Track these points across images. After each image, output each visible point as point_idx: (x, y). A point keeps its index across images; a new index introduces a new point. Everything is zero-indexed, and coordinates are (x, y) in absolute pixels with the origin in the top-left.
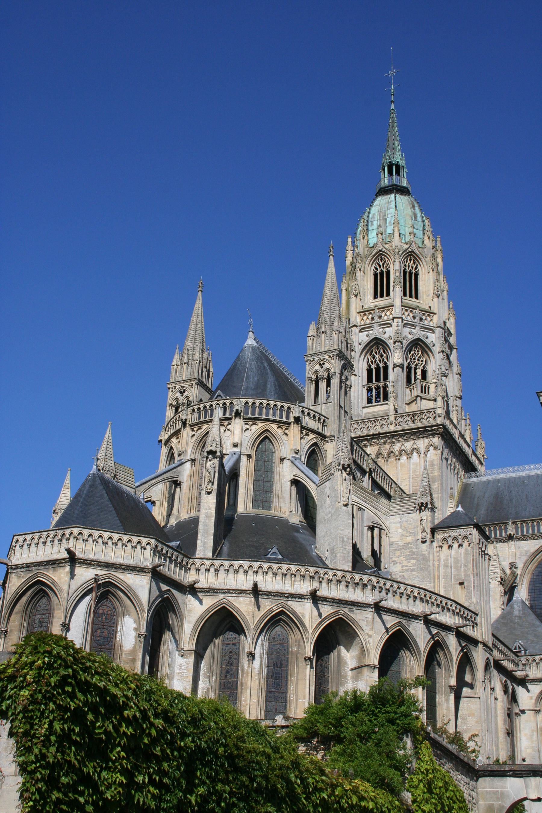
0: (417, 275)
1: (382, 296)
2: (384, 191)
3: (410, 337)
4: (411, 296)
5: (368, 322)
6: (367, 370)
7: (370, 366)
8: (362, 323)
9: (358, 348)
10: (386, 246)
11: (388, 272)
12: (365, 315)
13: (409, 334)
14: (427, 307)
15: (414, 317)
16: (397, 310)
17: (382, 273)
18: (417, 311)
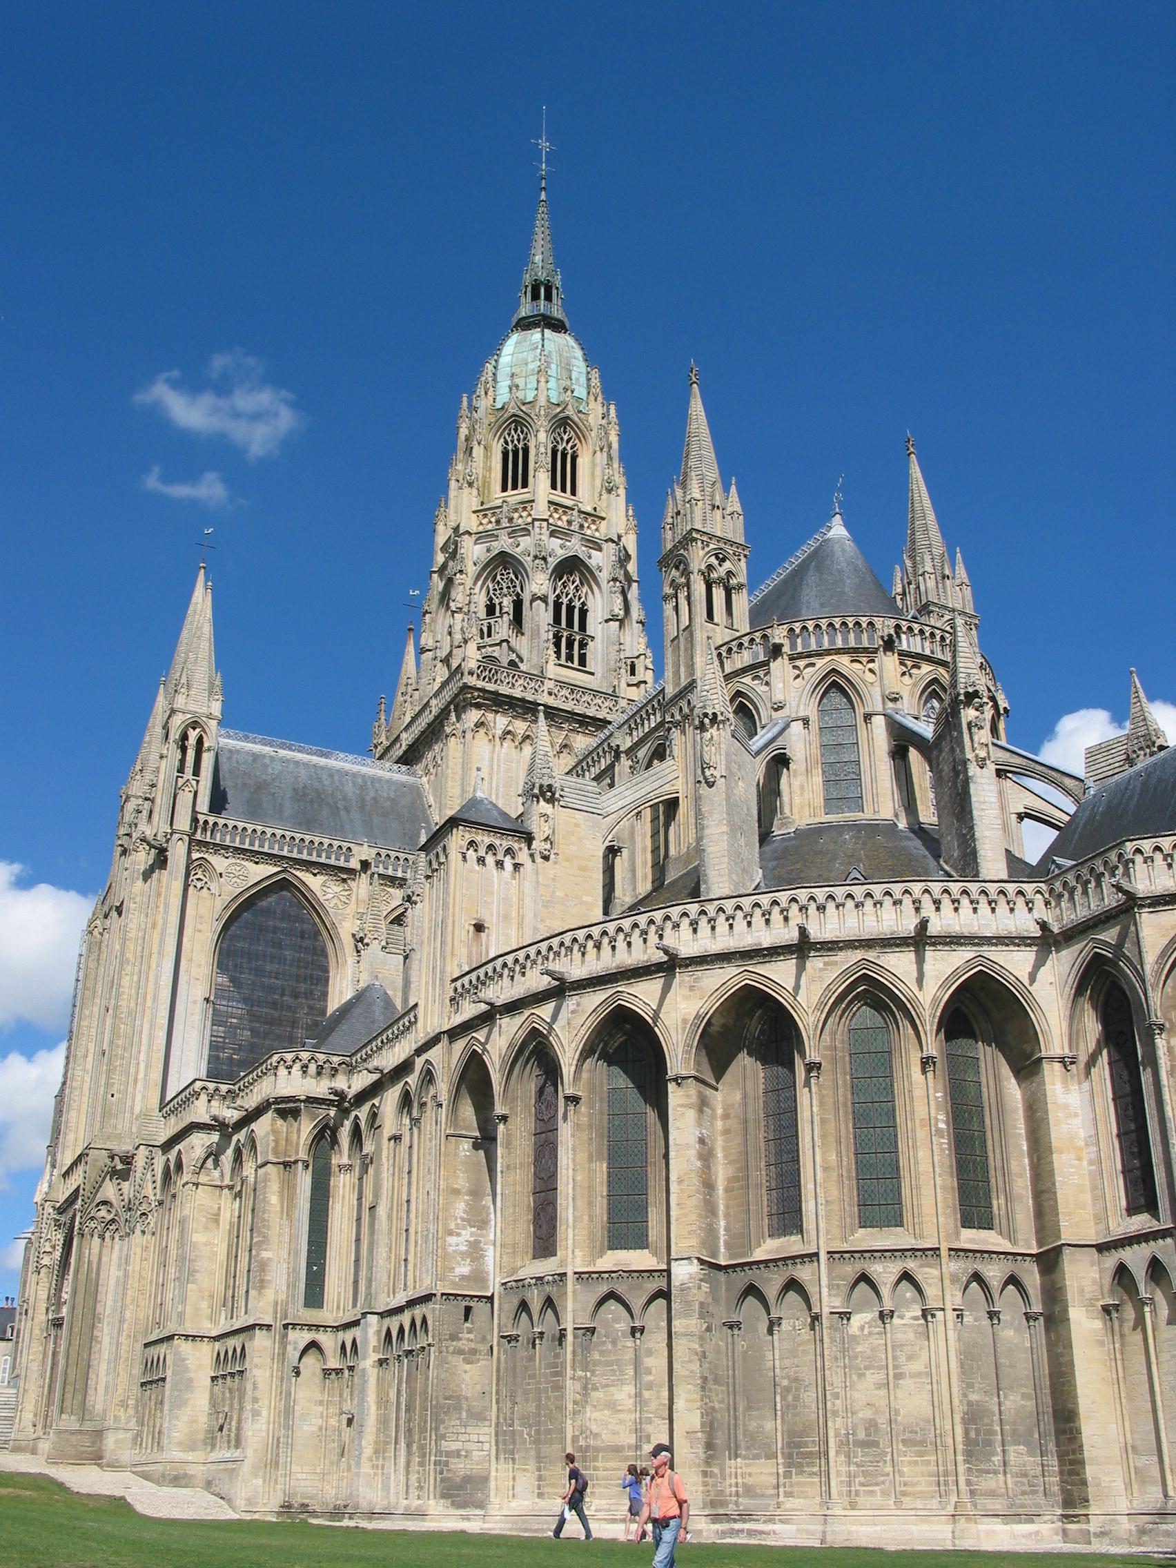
0: (574, 458)
1: (515, 487)
2: (525, 324)
4: (564, 490)
5: (490, 527)
7: (491, 599)
8: (481, 528)
9: (472, 570)
10: (523, 408)
11: (526, 450)
12: (485, 516)
13: (558, 549)
14: (589, 509)
15: (570, 523)
16: (541, 509)
18: (575, 513)
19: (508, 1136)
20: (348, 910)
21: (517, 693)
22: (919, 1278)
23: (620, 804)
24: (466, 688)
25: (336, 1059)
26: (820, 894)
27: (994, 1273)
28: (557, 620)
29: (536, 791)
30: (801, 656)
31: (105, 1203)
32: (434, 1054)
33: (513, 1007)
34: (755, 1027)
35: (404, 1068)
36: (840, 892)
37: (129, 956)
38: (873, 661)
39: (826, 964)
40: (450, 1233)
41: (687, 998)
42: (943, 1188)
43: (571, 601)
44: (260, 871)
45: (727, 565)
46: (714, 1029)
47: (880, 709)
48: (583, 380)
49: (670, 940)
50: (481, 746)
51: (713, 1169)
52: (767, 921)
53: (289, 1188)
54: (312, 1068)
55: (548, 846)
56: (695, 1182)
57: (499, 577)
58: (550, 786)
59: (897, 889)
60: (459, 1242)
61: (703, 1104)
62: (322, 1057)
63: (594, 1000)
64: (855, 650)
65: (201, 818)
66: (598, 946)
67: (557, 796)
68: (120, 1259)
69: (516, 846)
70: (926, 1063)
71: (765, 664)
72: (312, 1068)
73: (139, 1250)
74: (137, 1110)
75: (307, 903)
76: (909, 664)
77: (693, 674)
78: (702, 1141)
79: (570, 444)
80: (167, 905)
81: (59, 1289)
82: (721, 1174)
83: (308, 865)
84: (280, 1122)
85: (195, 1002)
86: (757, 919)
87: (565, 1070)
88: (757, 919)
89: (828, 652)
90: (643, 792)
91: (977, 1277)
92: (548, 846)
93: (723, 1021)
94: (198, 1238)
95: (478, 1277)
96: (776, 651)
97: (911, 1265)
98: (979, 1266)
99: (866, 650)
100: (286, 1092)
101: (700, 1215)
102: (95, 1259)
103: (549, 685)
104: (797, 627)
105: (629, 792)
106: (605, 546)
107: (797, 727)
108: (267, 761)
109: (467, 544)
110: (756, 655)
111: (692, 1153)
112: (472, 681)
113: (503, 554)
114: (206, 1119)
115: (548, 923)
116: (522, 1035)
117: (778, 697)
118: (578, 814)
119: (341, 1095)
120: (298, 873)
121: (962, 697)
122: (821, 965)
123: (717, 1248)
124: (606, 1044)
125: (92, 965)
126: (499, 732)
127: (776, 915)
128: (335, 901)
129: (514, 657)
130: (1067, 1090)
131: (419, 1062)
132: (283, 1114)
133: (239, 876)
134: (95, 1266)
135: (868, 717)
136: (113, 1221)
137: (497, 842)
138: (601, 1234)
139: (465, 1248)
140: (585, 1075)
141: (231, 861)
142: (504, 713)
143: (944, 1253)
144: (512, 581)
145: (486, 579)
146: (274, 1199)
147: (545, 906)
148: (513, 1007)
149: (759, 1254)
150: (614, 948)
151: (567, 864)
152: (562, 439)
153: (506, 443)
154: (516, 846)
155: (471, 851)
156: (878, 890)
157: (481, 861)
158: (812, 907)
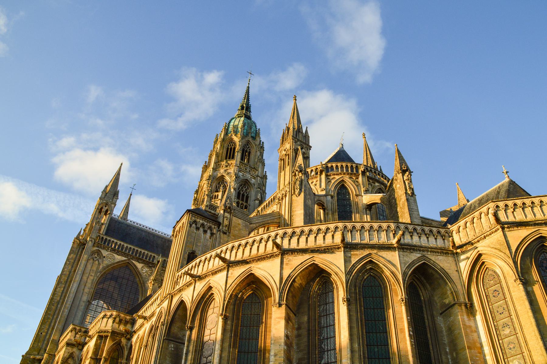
25: (128, 317)
34: (315, 287)
44: (119, 258)
46: (296, 285)
55: (227, 229)
61: (288, 319)
62: (122, 315)
65: (101, 236)
67: (232, 211)
69: (213, 226)
72: (118, 320)
83: (138, 260)
85: (84, 302)
93: (300, 282)
120: (134, 262)
124: (243, 294)
137: (206, 223)
154: (213, 226)
155: (194, 225)
157: (198, 229)
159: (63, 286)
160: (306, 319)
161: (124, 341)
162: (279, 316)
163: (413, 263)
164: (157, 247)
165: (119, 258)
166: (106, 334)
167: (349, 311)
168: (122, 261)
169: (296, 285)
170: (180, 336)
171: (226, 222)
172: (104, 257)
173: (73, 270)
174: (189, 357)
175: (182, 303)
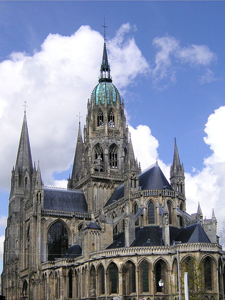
0: (114, 117)
3: (111, 142)
6: (96, 155)
11: (103, 116)
17: (100, 116)
18: (114, 133)
19: (97, 277)
20: (71, 225)
21: (102, 178)
22: (150, 299)
23: (116, 221)
24: (91, 177)
25: (72, 259)
26: (139, 248)
27: (161, 298)
28: (110, 158)
29: (102, 221)
30: (145, 197)
31: (33, 280)
32: (87, 263)
33: (98, 259)
35: (83, 264)
36: (142, 248)
37: (32, 236)
38: (158, 197)
39: (139, 258)
40: (91, 290)
41: (121, 261)
42: (154, 287)
43: (113, 153)
44: (54, 219)
45: (135, 176)
47: (158, 206)
48: (115, 97)
49: (119, 253)
50: (96, 189)
51: (125, 283)
52: (132, 251)
53: (65, 280)
54: (68, 261)
55: (104, 230)
56: (122, 286)
57: (98, 148)
58: (104, 221)
59: (150, 248)
60: (92, 291)
61: (123, 276)
62: (69, 259)
63: (109, 260)
64: (155, 196)
65: (43, 210)
66: (109, 253)
67: (105, 222)
68: (36, 289)
70: (152, 271)
71: (140, 197)
72: (68, 261)
73: (40, 288)
74: (37, 263)
75: (63, 224)
76: (164, 197)
77: (128, 197)
78: (123, 280)
79: (112, 114)
80: (38, 228)
81: (23, 292)
82: (127, 284)
83: (63, 217)
84: (64, 270)
85: (45, 244)
86: (131, 251)
87: (105, 269)
88: (131, 251)
89: (150, 196)
90: (120, 218)
91: (158, 298)
92: (104, 230)
94: (51, 286)
95: (95, 296)
96: (142, 195)
97: (149, 297)
98: (159, 297)
99: (156, 196)
100: (64, 265)
101: (122, 290)
102: (32, 289)
103: (109, 175)
104: (145, 191)
105: (118, 219)
106: (120, 140)
107: (145, 209)
108: (52, 192)
109: (90, 140)
110: (138, 196)
111: (122, 282)
112: (93, 176)
113: (98, 143)
114: (50, 267)
115: (104, 243)
116: (100, 263)
117: (142, 204)
118: (109, 224)
119: (73, 265)
120: (61, 219)
121: (165, 214)
122: (139, 258)
123: (126, 294)
125: (21, 232)
126: (99, 186)
127: (133, 251)
128: (69, 223)
129: (102, 168)
130: (171, 274)
131: (85, 264)
132: (63, 268)
133: (50, 220)
134: (32, 290)
135: (156, 208)
136: (34, 283)
138: (111, 291)
139: (93, 292)
140: (108, 270)
141: (49, 218)
142: (100, 182)
143: (153, 296)
144: (101, 149)
145: (95, 148)
146: (63, 282)
147: (104, 240)
148: (98, 259)
149: (131, 295)
150: (111, 253)
151: (107, 233)
152: (111, 113)
153: (98, 114)
155: (92, 233)
156: (147, 248)
157: (93, 234)
158: (138, 250)
159: (34, 239)
160: (128, 274)
161: (72, 268)
162: (121, 275)
163: (157, 259)
164: (69, 202)
165: (54, 219)
166: (65, 267)
167: (138, 274)
168: (56, 220)
169: (125, 265)
170: (94, 274)
171: (103, 228)
172: (47, 220)
173: (35, 231)
174: (98, 283)
175: (93, 266)
